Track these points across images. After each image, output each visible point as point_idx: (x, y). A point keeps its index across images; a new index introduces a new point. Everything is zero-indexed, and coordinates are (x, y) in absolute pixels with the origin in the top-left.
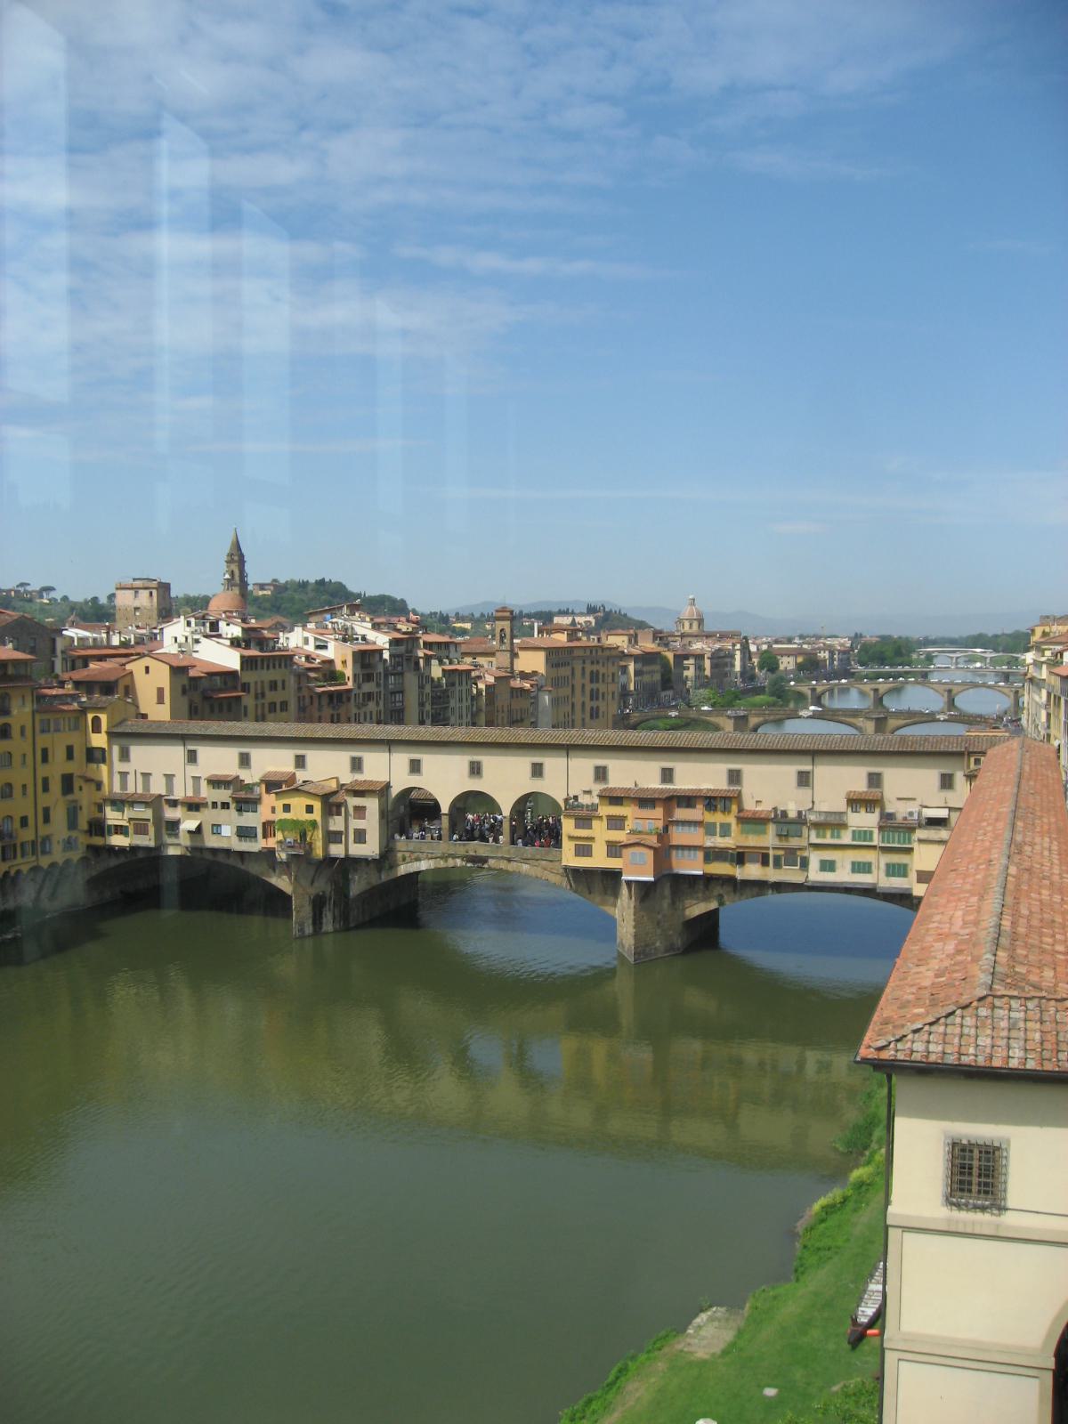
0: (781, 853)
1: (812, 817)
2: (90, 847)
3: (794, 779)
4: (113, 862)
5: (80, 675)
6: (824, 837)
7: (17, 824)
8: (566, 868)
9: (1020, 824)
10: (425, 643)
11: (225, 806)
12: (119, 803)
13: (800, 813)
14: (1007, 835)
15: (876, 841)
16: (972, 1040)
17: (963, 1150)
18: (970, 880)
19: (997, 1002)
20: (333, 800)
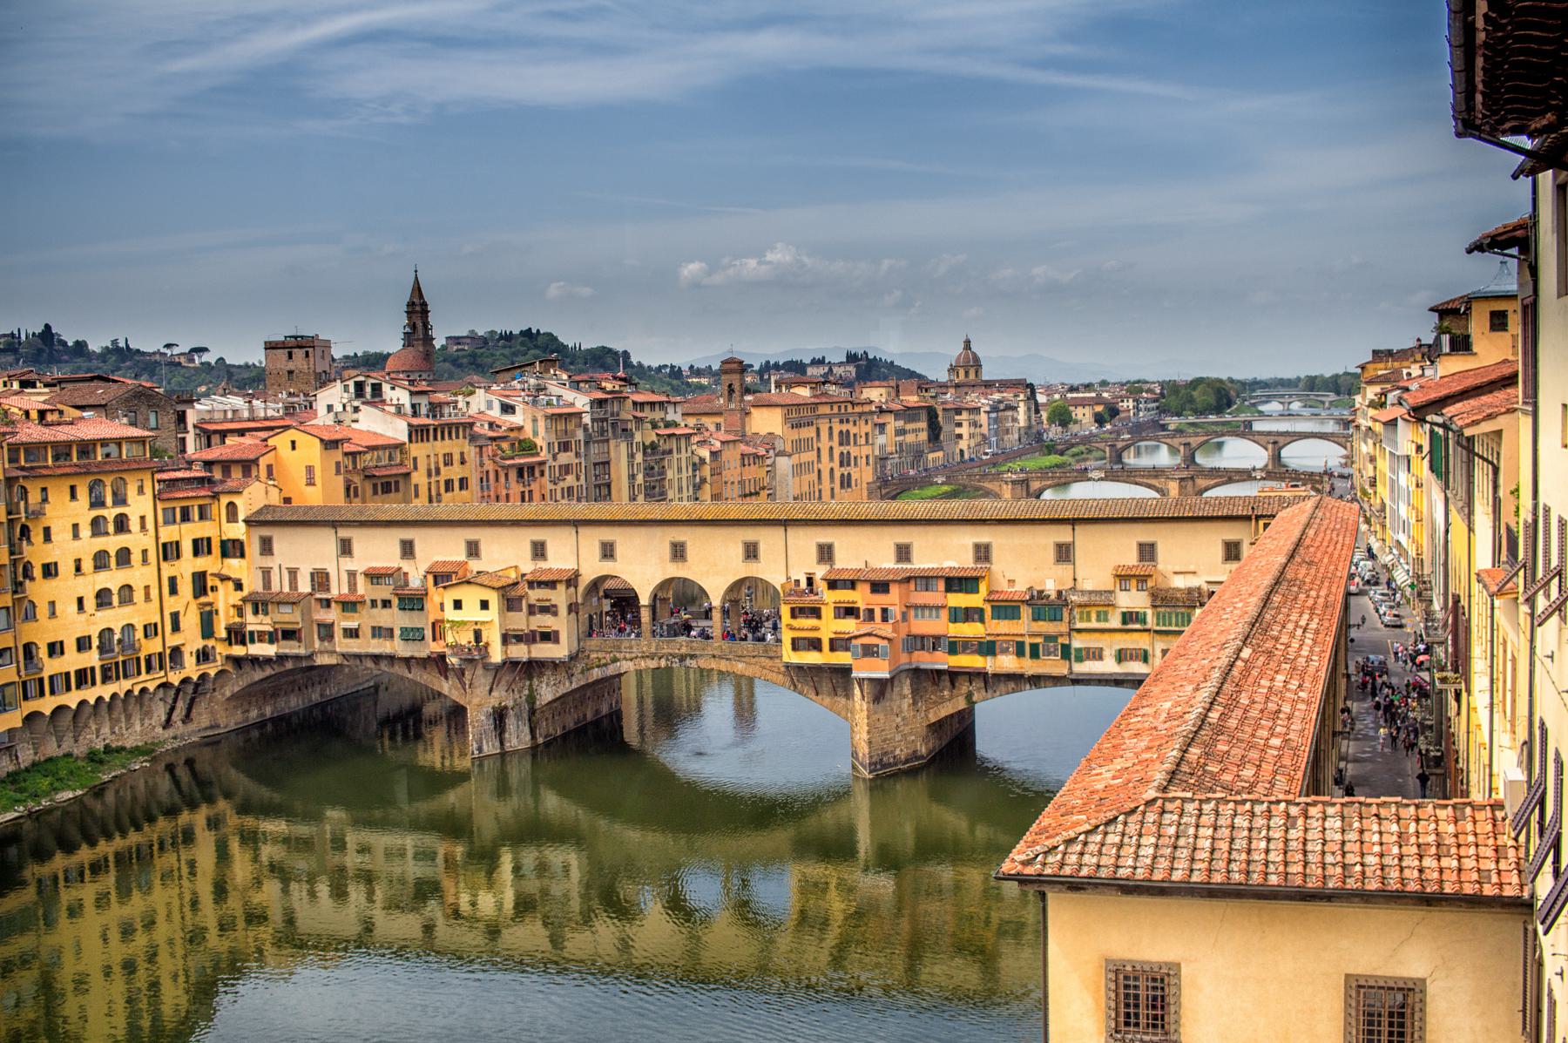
0: (1039, 640)
1: (1074, 598)
2: (228, 658)
3: (1051, 554)
4: (258, 675)
5: (214, 453)
6: (1089, 620)
7: (140, 634)
8: (788, 666)
9: (1277, 599)
10: (635, 403)
11: (386, 604)
12: (259, 604)
13: (1059, 593)
14: (1252, 610)
15: (1148, 626)
16: (1132, 850)
17: (1126, 978)
18: (1195, 666)
19: (1169, 806)
20: (513, 594)
